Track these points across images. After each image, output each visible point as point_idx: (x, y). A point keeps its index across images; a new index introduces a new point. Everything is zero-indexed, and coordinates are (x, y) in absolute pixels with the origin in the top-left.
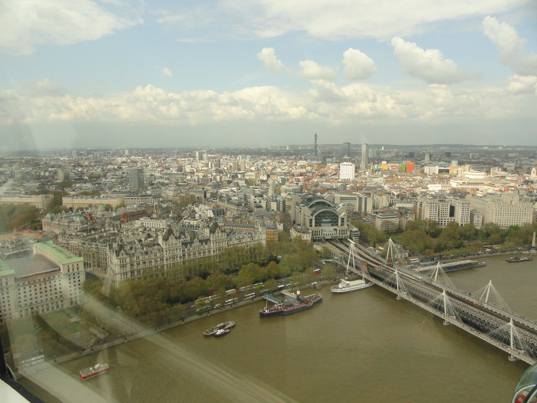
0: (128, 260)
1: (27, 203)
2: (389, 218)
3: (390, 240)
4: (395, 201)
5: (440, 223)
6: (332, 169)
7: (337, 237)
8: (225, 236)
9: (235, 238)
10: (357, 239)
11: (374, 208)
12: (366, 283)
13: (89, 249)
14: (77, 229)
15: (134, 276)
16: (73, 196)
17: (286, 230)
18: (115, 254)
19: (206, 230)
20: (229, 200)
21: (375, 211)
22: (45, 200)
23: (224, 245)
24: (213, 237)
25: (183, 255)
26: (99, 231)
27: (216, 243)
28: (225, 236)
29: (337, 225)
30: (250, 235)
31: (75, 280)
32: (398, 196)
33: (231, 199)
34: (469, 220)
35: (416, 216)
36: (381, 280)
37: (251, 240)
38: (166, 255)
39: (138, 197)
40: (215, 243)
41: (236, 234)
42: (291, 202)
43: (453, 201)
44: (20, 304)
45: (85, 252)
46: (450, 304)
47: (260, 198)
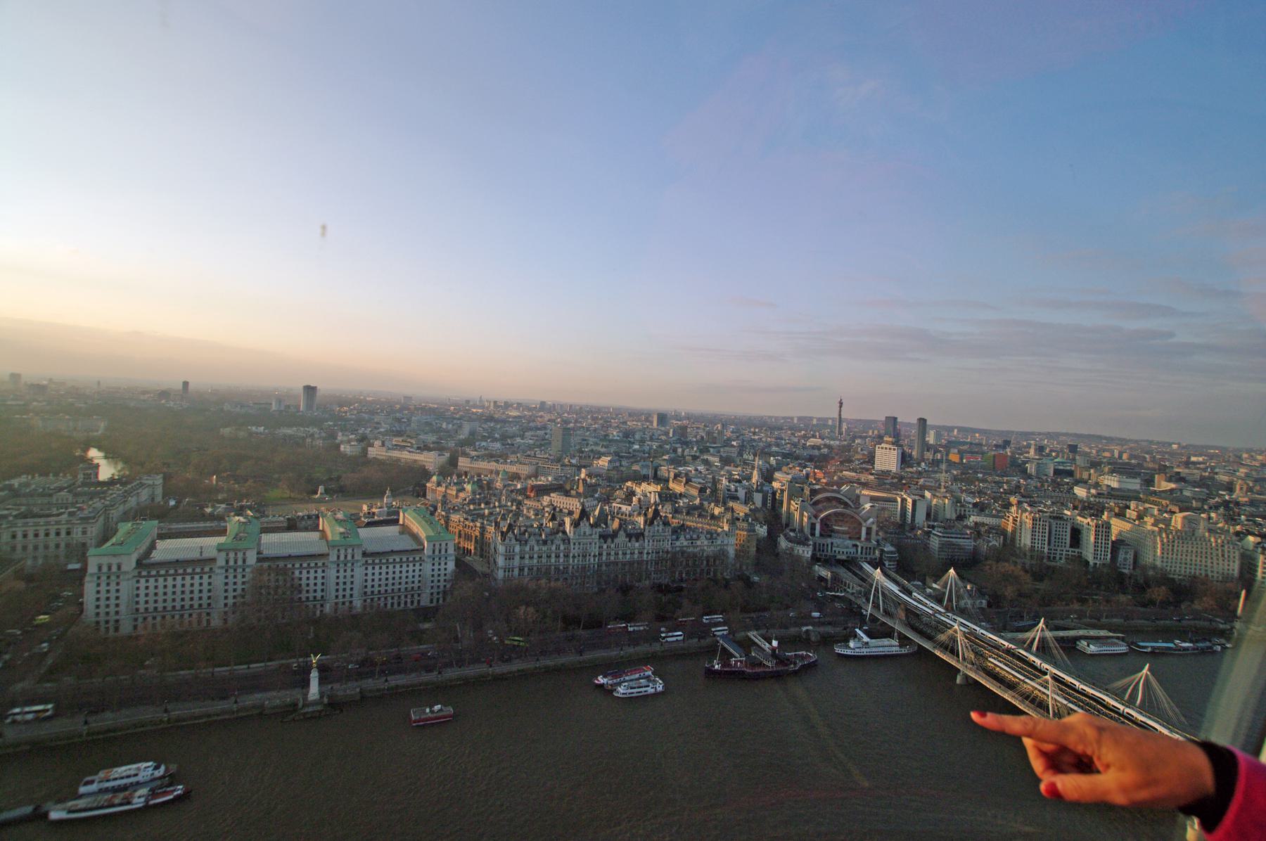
0: (517, 549)
1: (415, 461)
3: (952, 571)
5: (1052, 556)
6: (864, 454)
9: (685, 537)
10: (893, 565)
23: (667, 546)
24: (649, 531)
25: (599, 554)
26: (492, 505)
27: (653, 541)
29: (859, 538)
30: (709, 536)
31: (440, 567)
34: (1109, 556)
35: (1005, 540)
38: (574, 550)
40: (651, 541)
41: (687, 531)
44: (366, 590)
47: (737, 484)
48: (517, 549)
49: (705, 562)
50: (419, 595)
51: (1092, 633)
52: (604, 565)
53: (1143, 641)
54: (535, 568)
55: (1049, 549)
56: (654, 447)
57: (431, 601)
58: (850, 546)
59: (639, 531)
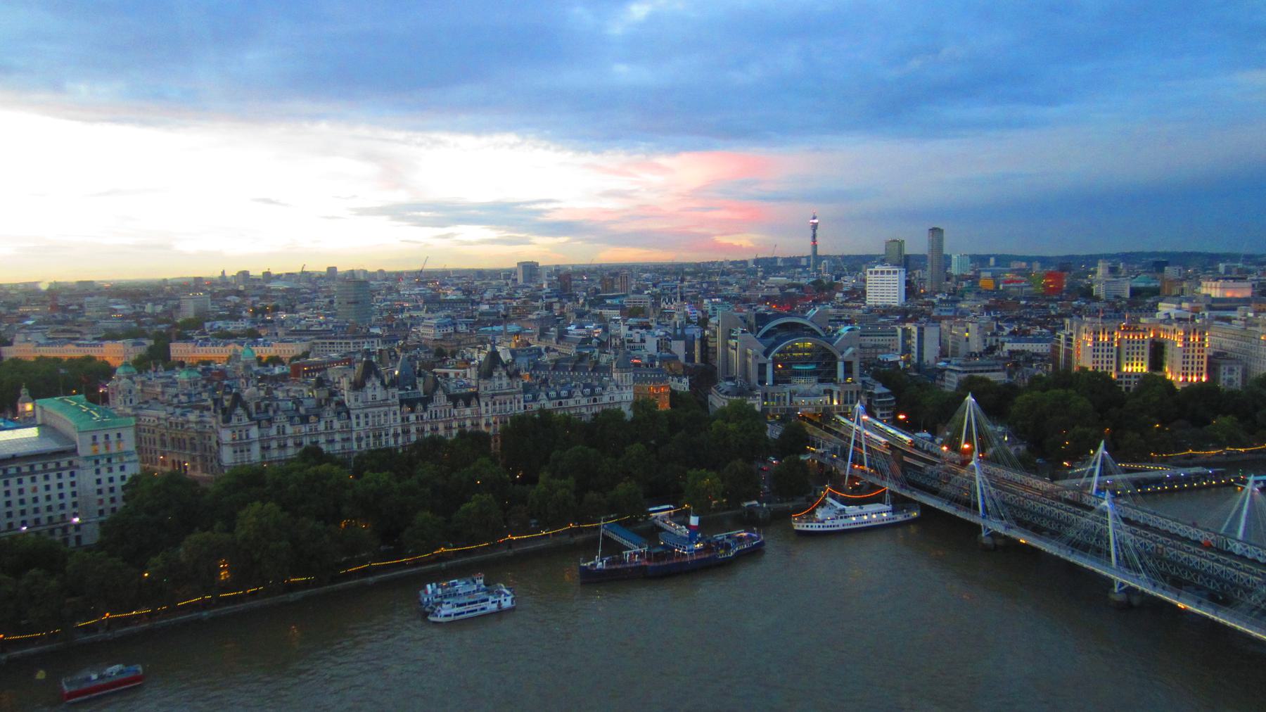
3: (970, 399)
5: (1124, 386)
8: (518, 386)
9: (547, 395)
10: (888, 415)
12: (894, 511)
16: (197, 341)
18: (220, 417)
22: (131, 350)
25: (403, 432)
27: (494, 404)
30: (587, 391)
32: (1012, 333)
35: (1056, 367)
37: (592, 403)
38: (359, 427)
45: (174, 435)
47: (643, 331)
48: (254, 432)
55: (1118, 377)
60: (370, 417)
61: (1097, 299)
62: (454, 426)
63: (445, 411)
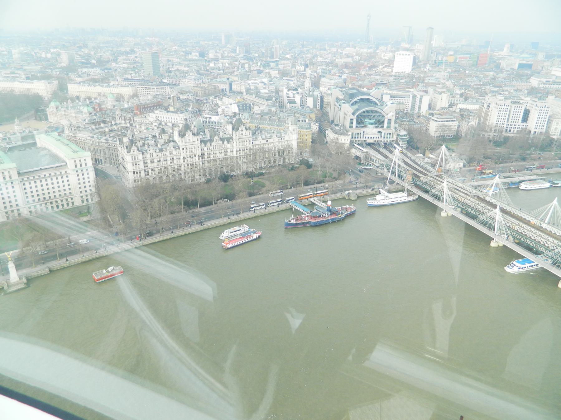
1: (28, 90)
2: (447, 121)
3: (444, 147)
4: (457, 101)
5: (508, 129)
6: (385, 60)
7: (381, 141)
9: (262, 137)
10: (405, 144)
11: (430, 108)
13: (99, 144)
14: (85, 120)
15: (148, 175)
16: (79, 83)
17: (322, 132)
18: (126, 150)
19: (228, 126)
20: (258, 94)
21: (431, 112)
24: (236, 136)
25: (202, 155)
26: (110, 124)
27: (240, 142)
28: (250, 134)
29: (383, 127)
30: (278, 135)
32: (462, 95)
33: (259, 92)
34: (545, 127)
35: (479, 120)
36: (427, 192)
37: (280, 140)
38: (184, 153)
39: (153, 86)
40: (238, 142)
41: (263, 132)
42: (330, 98)
43: (530, 103)
44: (28, 200)
45: (94, 147)
46: (503, 223)
47: (295, 92)
48: (141, 157)
49: (277, 154)
50: (72, 199)
51: (528, 178)
52: (206, 162)
53: (557, 180)
54: (156, 170)
55: (507, 125)
56: (227, 65)
57: (83, 201)
58: (377, 133)
59: (229, 136)
60: (188, 149)
61: (502, 70)
62: (223, 152)
63: (219, 145)
